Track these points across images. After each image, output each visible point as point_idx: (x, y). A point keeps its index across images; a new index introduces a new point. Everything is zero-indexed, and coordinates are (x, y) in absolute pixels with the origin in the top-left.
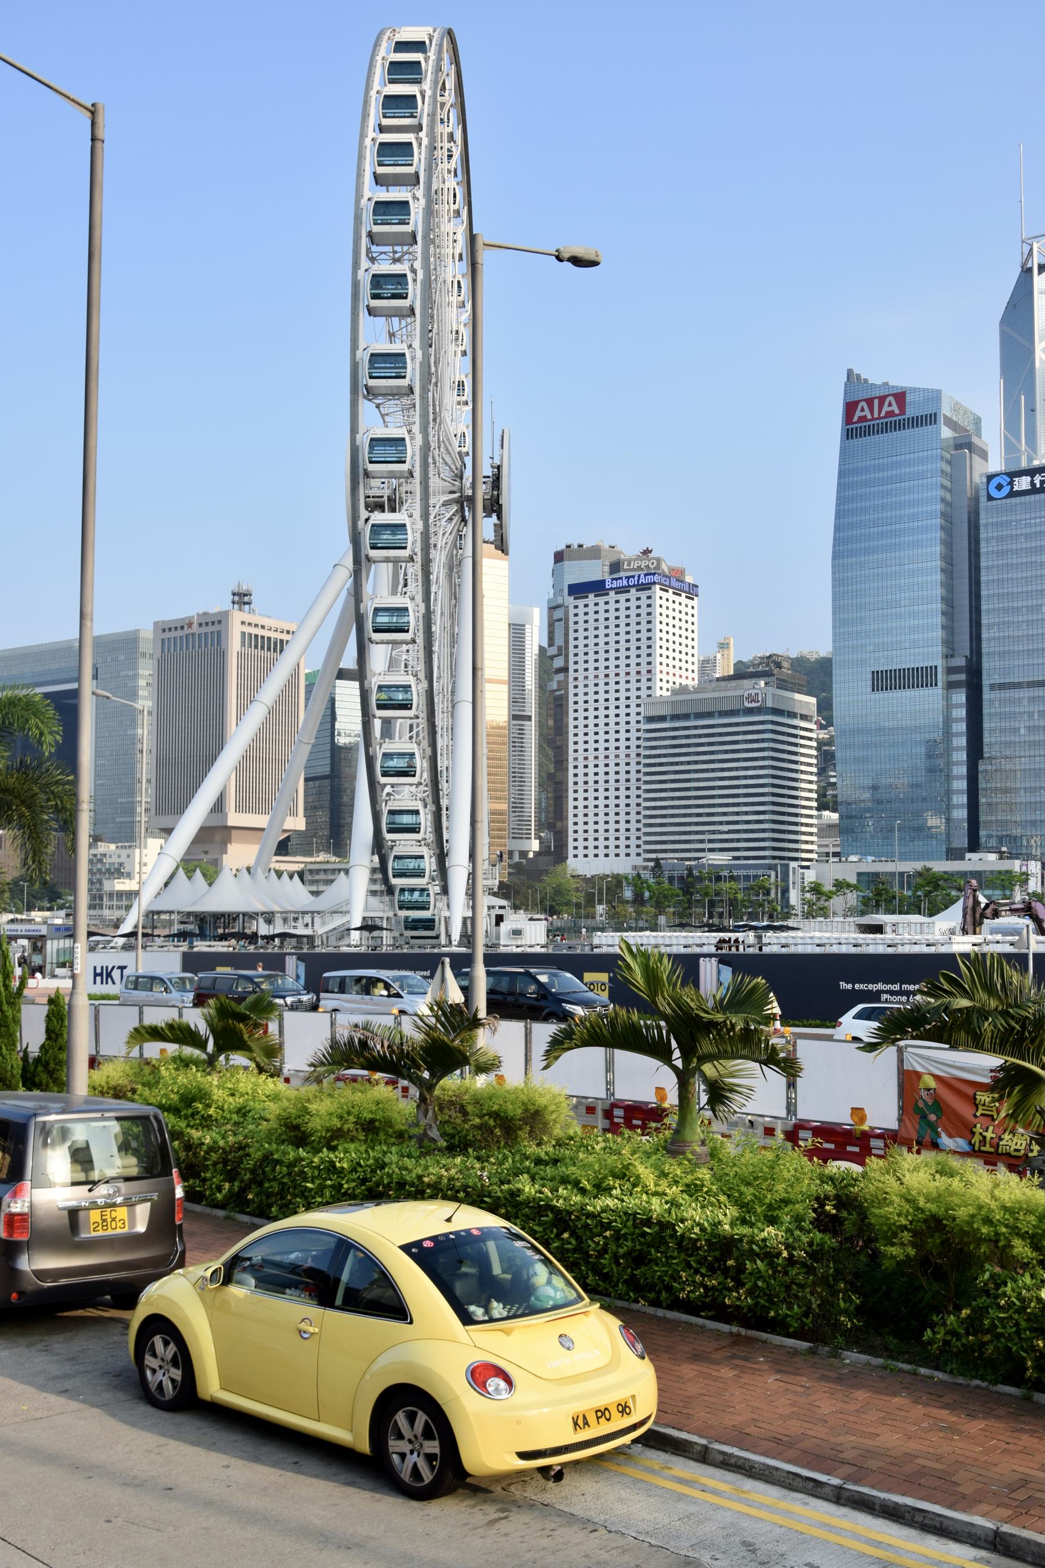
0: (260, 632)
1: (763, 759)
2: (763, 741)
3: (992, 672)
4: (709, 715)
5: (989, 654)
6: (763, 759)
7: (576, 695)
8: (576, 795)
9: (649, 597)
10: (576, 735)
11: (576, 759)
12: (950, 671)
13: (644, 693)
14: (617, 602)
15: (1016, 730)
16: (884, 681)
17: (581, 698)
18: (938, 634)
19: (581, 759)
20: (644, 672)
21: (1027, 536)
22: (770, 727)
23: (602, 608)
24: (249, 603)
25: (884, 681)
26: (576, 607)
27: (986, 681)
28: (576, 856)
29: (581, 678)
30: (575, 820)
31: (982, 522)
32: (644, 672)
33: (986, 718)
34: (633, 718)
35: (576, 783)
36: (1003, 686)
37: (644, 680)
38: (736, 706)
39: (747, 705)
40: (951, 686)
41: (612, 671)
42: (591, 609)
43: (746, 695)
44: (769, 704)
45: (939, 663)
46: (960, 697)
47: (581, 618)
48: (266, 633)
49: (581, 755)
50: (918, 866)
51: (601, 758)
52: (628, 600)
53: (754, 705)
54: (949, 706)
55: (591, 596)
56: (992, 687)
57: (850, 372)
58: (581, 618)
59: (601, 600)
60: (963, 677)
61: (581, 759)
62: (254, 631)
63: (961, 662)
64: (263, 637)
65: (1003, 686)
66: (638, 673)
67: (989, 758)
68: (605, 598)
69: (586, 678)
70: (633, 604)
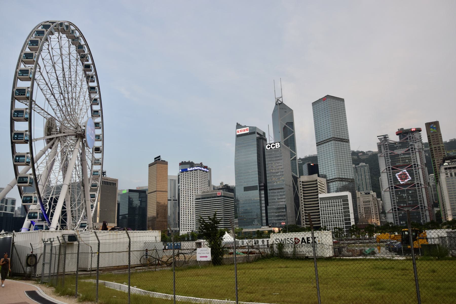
0: (107, 181)
1: (222, 207)
2: (221, 203)
3: (269, 186)
4: (210, 198)
5: (268, 182)
6: (222, 207)
7: (181, 194)
8: (182, 217)
9: (197, 172)
10: (181, 203)
11: (181, 208)
12: (260, 186)
13: (196, 193)
14: (190, 173)
15: (275, 199)
16: (247, 189)
17: (182, 195)
18: (257, 179)
19: (183, 208)
20: (196, 189)
21: (275, 157)
22: (223, 200)
23: (187, 175)
24: (105, 174)
25: (247, 189)
26: (181, 175)
27: (268, 189)
28: (182, 231)
29: (182, 190)
30: (181, 222)
31: (266, 154)
32: (196, 189)
33: (268, 197)
34: (194, 199)
35: (181, 214)
36: (272, 189)
37: (196, 190)
38: (215, 196)
39: (218, 195)
40: (260, 190)
41: (189, 188)
42: (185, 175)
43: (218, 193)
44: (223, 195)
45: (258, 185)
46: (263, 192)
47: (182, 177)
48: (108, 181)
49: (183, 207)
50: (257, 229)
51: (187, 208)
52: (192, 173)
53: (219, 195)
54: (260, 194)
55: (185, 172)
56: (270, 190)
57: (237, 123)
58: (182, 177)
59: (187, 173)
60: (263, 188)
61: (183, 208)
62: (105, 180)
63: (263, 184)
64: (108, 182)
65: (272, 189)
66: (195, 189)
67: (270, 205)
68: (188, 172)
69: (184, 190)
70: (194, 174)
